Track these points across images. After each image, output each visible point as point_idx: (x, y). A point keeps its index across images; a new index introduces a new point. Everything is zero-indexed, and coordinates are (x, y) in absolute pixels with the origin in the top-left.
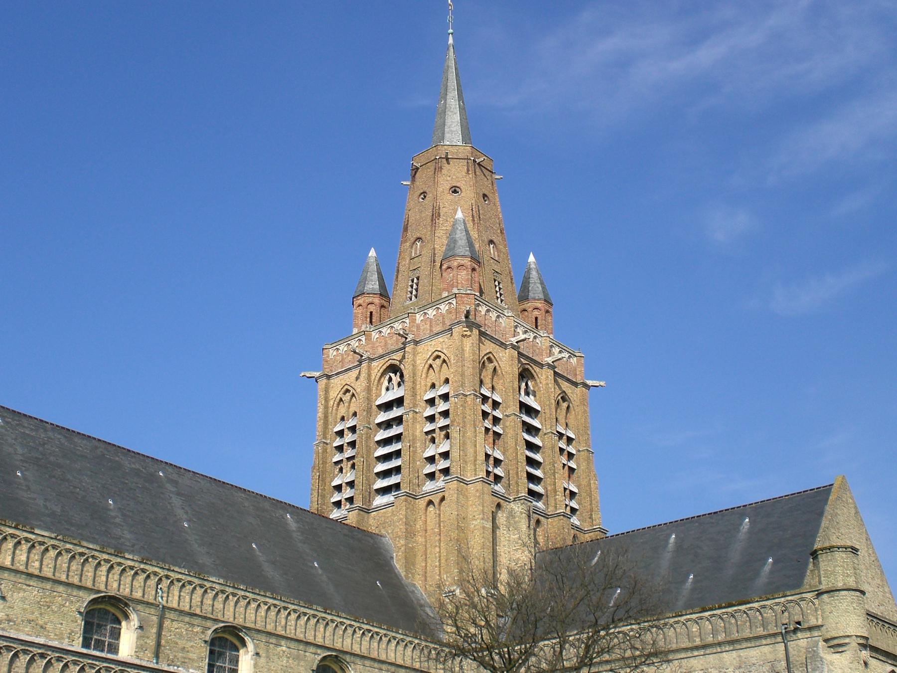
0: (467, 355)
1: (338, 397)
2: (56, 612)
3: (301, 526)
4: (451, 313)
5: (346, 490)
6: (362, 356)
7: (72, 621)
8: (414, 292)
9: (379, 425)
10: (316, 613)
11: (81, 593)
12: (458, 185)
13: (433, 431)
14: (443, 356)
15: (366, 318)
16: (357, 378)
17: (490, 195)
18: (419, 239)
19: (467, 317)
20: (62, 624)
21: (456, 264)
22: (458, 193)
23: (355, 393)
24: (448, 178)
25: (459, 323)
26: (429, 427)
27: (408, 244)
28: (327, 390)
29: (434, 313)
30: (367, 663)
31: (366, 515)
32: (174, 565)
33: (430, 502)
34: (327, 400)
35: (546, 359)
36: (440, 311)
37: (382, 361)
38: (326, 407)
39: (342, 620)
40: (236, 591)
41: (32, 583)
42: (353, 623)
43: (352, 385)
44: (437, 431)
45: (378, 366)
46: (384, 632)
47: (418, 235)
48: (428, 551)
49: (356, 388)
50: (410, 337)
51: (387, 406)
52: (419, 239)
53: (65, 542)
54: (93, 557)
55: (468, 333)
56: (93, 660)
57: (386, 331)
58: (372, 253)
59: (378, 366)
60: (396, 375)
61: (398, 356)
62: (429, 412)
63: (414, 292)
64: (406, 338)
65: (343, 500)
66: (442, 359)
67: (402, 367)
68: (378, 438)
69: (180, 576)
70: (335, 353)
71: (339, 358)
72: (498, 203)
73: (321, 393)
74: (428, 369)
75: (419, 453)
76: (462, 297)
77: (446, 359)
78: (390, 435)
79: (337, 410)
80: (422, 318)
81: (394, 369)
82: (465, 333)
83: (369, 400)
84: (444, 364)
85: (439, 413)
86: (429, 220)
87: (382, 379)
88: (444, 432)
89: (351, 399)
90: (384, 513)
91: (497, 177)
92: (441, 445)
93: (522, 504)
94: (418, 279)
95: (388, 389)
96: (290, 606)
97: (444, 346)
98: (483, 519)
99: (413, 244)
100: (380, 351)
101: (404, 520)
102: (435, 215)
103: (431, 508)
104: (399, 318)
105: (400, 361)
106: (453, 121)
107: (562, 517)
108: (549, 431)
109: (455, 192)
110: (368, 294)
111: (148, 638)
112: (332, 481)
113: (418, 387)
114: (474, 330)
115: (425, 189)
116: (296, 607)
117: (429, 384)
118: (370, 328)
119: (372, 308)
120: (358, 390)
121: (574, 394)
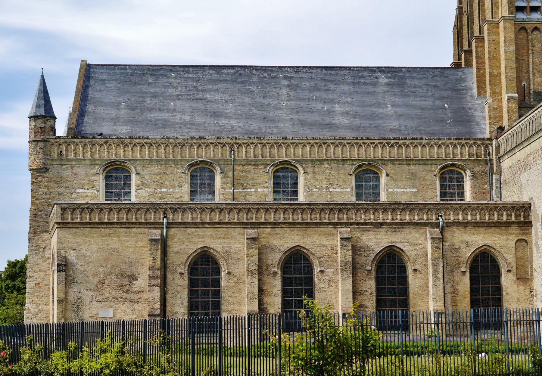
3: (392, 80)
7: (179, 177)
10: (349, 141)
20: (173, 180)
30: (397, 163)
39: (371, 141)
40: (286, 141)
41: (154, 163)
42: (381, 141)
46: (410, 141)
54: (187, 143)
69: (245, 141)
96: (328, 141)
111: (228, 177)
116: (333, 141)
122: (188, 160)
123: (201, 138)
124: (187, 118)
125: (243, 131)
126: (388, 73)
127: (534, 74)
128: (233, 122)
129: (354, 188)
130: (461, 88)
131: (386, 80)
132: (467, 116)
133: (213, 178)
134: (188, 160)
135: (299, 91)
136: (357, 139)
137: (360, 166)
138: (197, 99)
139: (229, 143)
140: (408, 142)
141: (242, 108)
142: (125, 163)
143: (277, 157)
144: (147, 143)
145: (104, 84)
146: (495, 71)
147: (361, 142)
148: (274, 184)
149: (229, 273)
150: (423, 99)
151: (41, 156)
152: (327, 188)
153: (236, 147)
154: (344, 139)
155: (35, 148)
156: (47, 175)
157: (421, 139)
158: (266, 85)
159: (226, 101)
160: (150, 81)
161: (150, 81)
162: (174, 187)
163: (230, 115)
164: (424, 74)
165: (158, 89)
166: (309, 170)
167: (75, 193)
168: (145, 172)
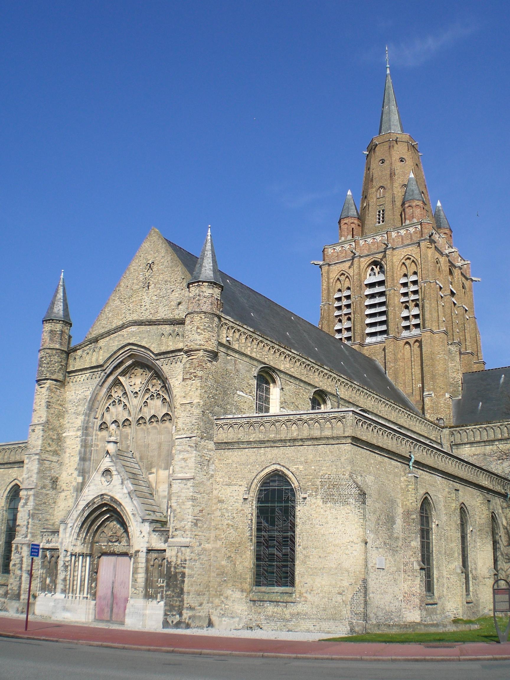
0: (429, 259)
1: (337, 277)
2: (301, 398)
4: (416, 233)
5: (344, 332)
6: (355, 254)
8: (381, 219)
9: (367, 296)
11: (309, 388)
12: (404, 157)
13: (408, 302)
14: (412, 258)
15: (350, 231)
16: (350, 267)
17: (419, 165)
18: (382, 187)
19: (430, 237)
21: (414, 204)
22: (403, 162)
23: (348, 275)
24: (398, 153)
25: (424, 240)
26: (403, 299)
27: (374, 189)
28: (328, 272)
29: (405, 232)
31: (362, 348)
32: (342, 374)
33: (407, 343)
34: (328, 278)
35: (457, 264)
36: (409, 231)
37: (368, 258)
38: (328, 283)
43: (346, 271)
44: (410, 302)
45: (365, 262)
47: (381, 185)
48: (406, 371)
49: (349, 273)
50: (390, 246)
51: (371, 285)
52: (382, 187)
53: (303, 357)
55: (430, 246)
56: (386, 428)
57: (370, 240)
58: (349, 193)
59: (365, 261)
60: (376, 268)
61: (380, 256)
62: (403, 290)
63: (381, 219)
64: (388, 246)
65: (343, 338)
66: (411, 260)
67: (383, 262)
68: (366, 304)
70: (332, 251)
71: (335, 254)
72: (422, 170)
73: (325, 274)
74: (402, 265)
75: (398, 314)
76: (425, 225)
77: (415, 260)
78: (376, 302)
79: (335, 285)
80: (396, 235)
81: (375, 263)
82: (429, 246)
83: (360, 281)
84: (413, 263)
85: (411, 291)
86: (388, 176)
87: (368, 269)
88: (414, 303)
89: (345, 279)
90: (374, 347)
91: (420, 154)
92: (413, 310)
93: (456, 346)
94: (383, 211)
95: (370, 275)
97: (413, 252)
98: (445, 354)
99: (378, 189)
100: (366, 253)
101: (393, 352)
102: (392, 175)
103: (407, 346)
104: (379, 234)
105: (381, 259)
106: (395, 117)
107: (470, 355)
108: (461, 305)
109: (402, 161)
110: (351, 217)
112: (334, 326)
113: (395, 275)
114: (433, 245)
115: (383, 158)
117: (402, 274)
118: (358, 238)
119: (353, 226)
120: (351, 274)
121: (467, 284)
142: (274, 372)
144: (289, 355)
149: (437, 525)
155: (211, 323)
156: (214, 363)
167: (237, 395)
168: (287, 388)
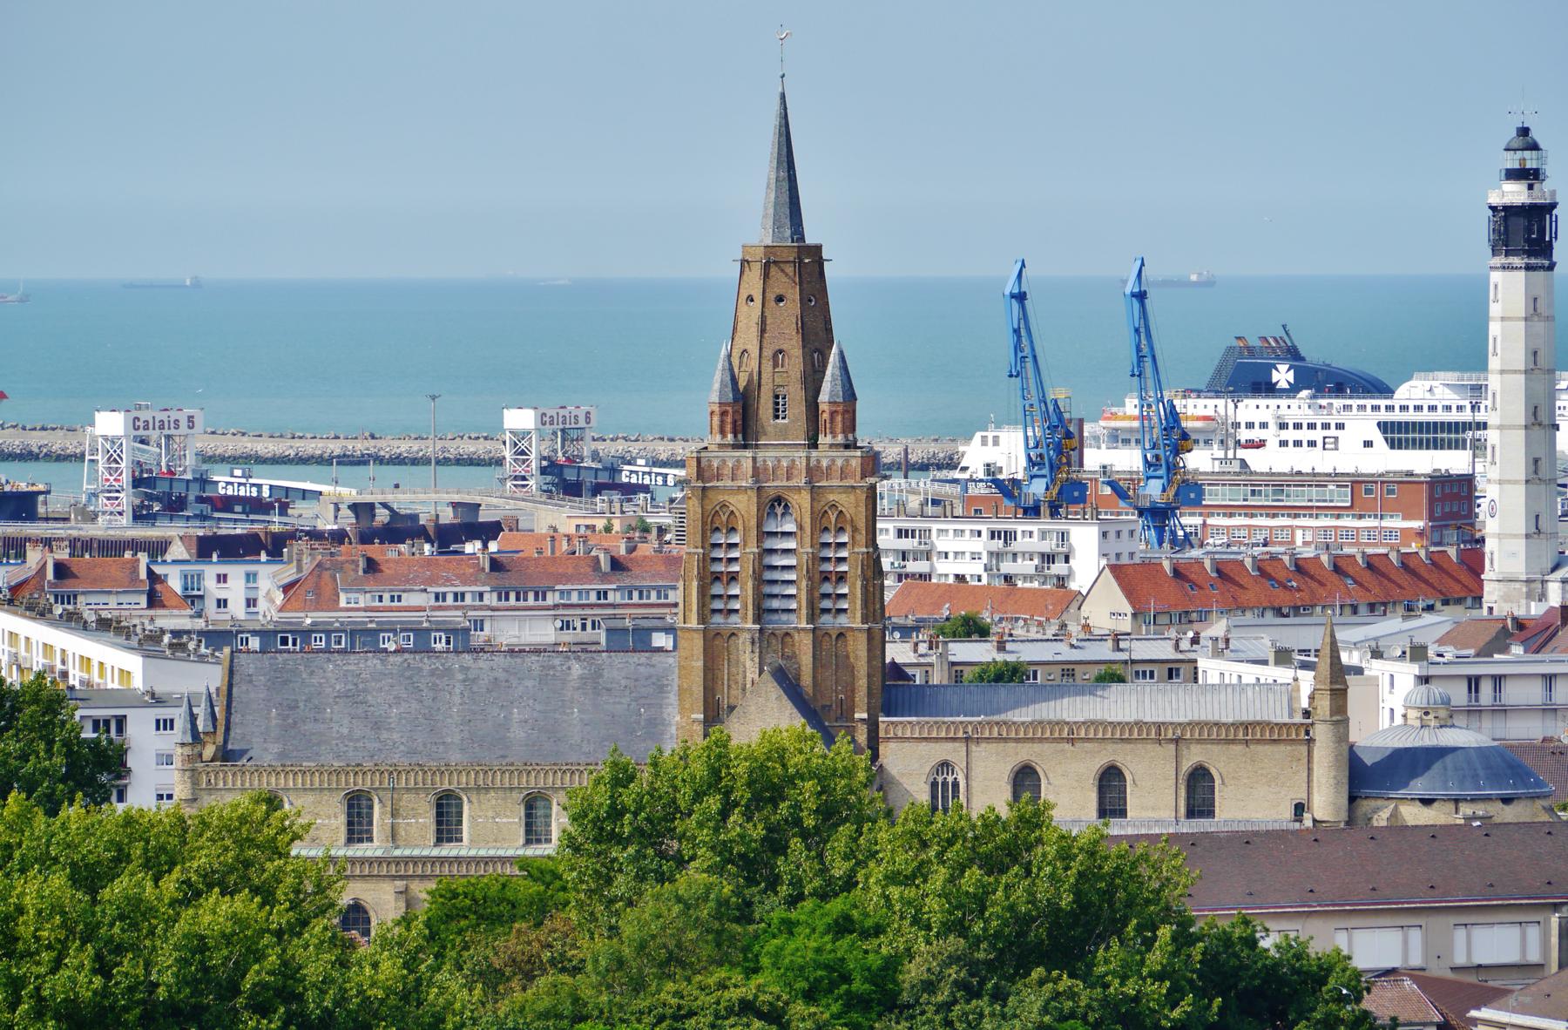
122: (344, 789)
123: (358, 765)
124: (345, 731)
125: (406, 749)
126: (584, 660)
127: (729, 686)
128: (395, 736)
129: (523, 818)
130: (666, 682)
131: (580, 672)
132: (663, 725)
133: (371, 807)
134: (344, 789)
135: (475, 689)
136: (526, 764)
137: (528, 794)
138: (356, 703)
139: (387, 770)
140: (582, 768)
141: (408, 716)
143: (439, 785)
145: (251, 682)
146: (685, 684)
147: (530, 768)
148: (437, 813)
150: (617, 700)
151: (189, 785)
152: (493, 818)
153: (395, 774)
154: (512, 764)
157: (597, 764)
158: (437, 681)
159: (390, 706)
160: (304, 676)
161: (304, 676)
162: (329, 817)
163: (392, 726)
164: (627, 662)
165: (312, 689)
166: (474, 799)
